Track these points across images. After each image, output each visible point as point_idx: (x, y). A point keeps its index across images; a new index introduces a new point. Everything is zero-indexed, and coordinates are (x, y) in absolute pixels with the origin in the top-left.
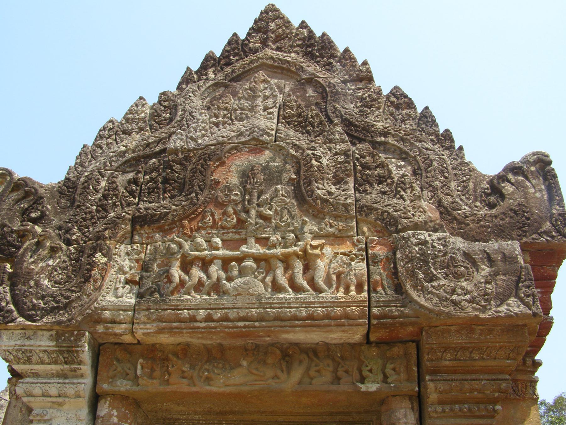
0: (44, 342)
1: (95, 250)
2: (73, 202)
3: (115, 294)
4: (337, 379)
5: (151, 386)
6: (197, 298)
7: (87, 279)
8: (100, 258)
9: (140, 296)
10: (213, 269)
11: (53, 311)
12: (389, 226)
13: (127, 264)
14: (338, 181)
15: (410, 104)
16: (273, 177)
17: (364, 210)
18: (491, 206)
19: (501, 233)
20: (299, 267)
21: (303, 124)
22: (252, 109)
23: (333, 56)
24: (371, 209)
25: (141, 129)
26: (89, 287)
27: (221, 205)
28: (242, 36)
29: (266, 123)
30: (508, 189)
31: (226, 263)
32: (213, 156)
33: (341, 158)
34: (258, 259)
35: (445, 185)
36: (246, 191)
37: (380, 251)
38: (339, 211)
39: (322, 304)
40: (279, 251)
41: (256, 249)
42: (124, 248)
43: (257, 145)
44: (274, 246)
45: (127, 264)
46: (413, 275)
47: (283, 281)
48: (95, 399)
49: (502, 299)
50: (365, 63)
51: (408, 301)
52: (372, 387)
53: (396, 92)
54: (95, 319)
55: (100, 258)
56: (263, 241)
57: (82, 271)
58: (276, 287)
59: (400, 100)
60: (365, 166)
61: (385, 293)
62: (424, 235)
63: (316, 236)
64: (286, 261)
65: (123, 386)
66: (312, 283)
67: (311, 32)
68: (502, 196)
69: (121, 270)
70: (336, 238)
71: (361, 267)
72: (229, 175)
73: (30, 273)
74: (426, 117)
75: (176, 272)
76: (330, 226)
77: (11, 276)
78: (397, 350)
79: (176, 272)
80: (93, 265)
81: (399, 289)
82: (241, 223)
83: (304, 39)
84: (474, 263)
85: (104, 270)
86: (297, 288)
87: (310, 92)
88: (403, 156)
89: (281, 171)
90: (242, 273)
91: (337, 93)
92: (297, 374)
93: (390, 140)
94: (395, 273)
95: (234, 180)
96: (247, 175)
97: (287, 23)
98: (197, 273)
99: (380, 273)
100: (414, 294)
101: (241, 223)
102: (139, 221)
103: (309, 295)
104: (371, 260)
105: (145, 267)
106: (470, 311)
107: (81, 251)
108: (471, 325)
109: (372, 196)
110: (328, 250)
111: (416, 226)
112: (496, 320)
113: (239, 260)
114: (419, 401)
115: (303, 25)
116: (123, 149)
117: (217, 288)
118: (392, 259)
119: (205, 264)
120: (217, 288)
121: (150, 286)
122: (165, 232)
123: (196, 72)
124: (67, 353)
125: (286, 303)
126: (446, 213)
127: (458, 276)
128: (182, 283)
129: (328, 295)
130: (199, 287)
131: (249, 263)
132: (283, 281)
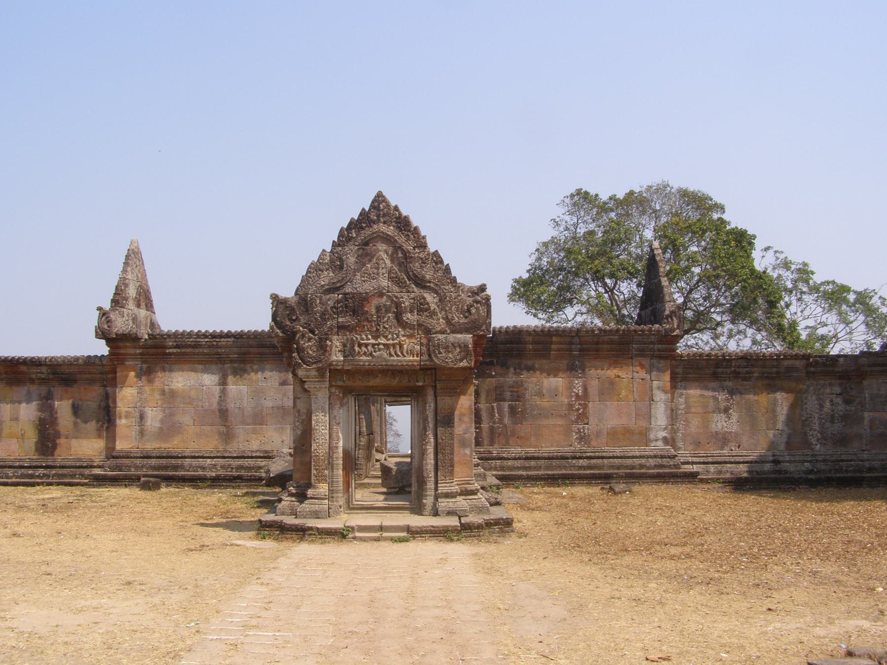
0: (314, 373)
1: (327, 339)
2: (307, 310)
3: (337, 357)
4: (409, 381)
5: (349, 383)
6: (364, 358)
7: (326, 351)
8: (328, 343)
9: (344, 357)
10: (369, 347)
11: (315, 363)
12: (428, 331)
13: (338, 344)
14: (411, 312)
15: (442, 262)
16: (388, 311)
17: (420, 325)
18: (466, 317)
19: (467, 331)
20: (398, 347)
21: (398, 282)
22: (378, 274)
23: (409, 231)
24: (422, 325)
25: (327, 269)
26: (327, 354)
27: (369, 322)
28: (367, 210)
29: (385, 283)
30: (473, 311)
31: (373, 345)
32: (364, 299)
33: (412, 301)
34: (384, 345)
35: (450, 309)
36: (378, 317)
37: (424, 341)
38: (412, 327)
39: (406, 361)
40: (391, 342)
41: (382, 341)
42: (335, 337)
43: (381, 295)
44: (388, 340)
45: (338, 344)
46: (434, 352)
47: (393, 353)
48: (331, 386)
49: (461, 360)
50: (424, 237)
51: (432, 360)
52: (421, 384)
53: (436, 254)
54: (331, 365)
55: (328, 343)
56: (386, 337)
57: (322, 347)
58: (391, 355)
59: (437, 258)
60: (421, 304)
61: (425, 357)
62: (440, 336)
63: (404, 336)
64: (394, 345)
65: (340, 383)
66: (402, 353)
67: (400, 214)
68: (470, 314)
69: (336, 347)
70: (410, 336)
71: (418, 347)
72: (371, 308)
73: (303, 348)
74: (447, 270)
75: (357, 348)
76: (409, 332)
77: (297, 349)
78: (429, 372)
79: (357, 348)
80: (327, 346)
81: (430, 356)
82: (377, 330)
83: (396, 218)
84: (455, 347)
85: (331, 347)
86: (398, 356)
87: (400, 255)
88: (436, 292)
89: (390, 307)
90: (380, 350)
91: (411, 257)
92: (397, 379)
93: (432, 285)
94: (428, 350)
95: (374, 311)
96: (378, 309)
97: (388, 205)
98: (364, 349)
99: (424, 348)
100: (434, 358)
101: (377, 330)
102: (341, 328)
103: (401, 358)
104: (421, 344)
105: (344, 345)
106: (451, 365)
107: (320, 339)
108: (452, 368)
109: (423, 319)
110: (407, 341)
111: (436, 333)
112: (458, 369)
113: (379, 344)
114: (435, 387)
115: (396, 208)
116: (323, 283)
117: (371, 354)
118: (428, 345)
119: (366, 345)
120: (371, 354)
121: (348, 351)
122: (351, 332)
123: (347, 230)
124: (322, 376)
125: (394, 360)
126: (448, 321)
127: (449, 352)
128: (359, 352)
129: (407, 358)
130: (365, 354)
131: (381, 347)
132: (393, 353)
